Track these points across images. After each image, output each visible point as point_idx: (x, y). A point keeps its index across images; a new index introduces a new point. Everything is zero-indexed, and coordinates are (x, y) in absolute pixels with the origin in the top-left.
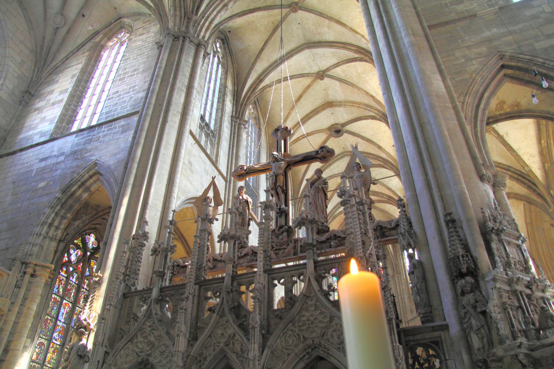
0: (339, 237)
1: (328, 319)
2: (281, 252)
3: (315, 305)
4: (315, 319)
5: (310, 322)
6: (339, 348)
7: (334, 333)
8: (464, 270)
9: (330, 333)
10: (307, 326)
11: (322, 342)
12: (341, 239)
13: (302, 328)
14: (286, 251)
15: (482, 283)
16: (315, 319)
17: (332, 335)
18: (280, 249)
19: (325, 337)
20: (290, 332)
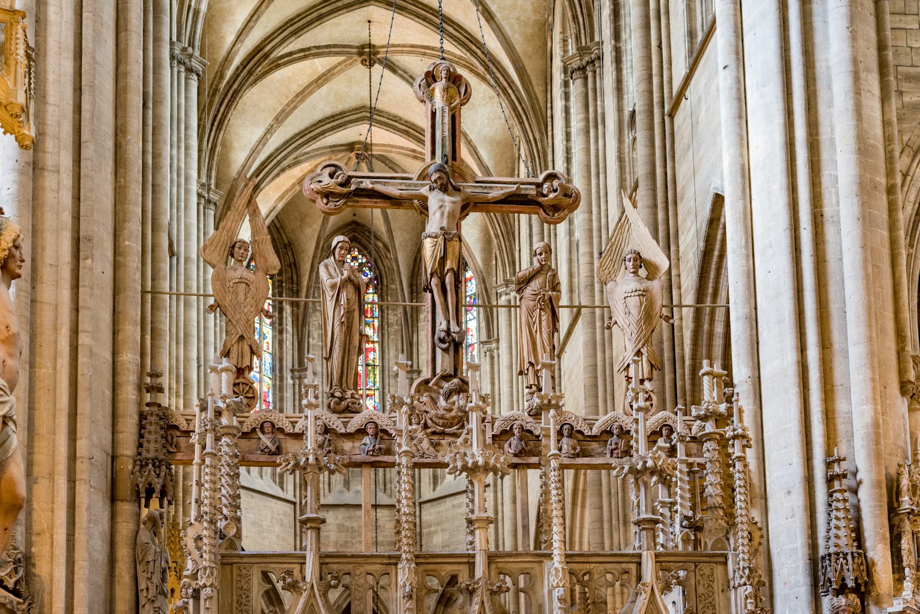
0: (580, 432)
2: (443, 442)
12: (580, 437)
18: (443, 434)
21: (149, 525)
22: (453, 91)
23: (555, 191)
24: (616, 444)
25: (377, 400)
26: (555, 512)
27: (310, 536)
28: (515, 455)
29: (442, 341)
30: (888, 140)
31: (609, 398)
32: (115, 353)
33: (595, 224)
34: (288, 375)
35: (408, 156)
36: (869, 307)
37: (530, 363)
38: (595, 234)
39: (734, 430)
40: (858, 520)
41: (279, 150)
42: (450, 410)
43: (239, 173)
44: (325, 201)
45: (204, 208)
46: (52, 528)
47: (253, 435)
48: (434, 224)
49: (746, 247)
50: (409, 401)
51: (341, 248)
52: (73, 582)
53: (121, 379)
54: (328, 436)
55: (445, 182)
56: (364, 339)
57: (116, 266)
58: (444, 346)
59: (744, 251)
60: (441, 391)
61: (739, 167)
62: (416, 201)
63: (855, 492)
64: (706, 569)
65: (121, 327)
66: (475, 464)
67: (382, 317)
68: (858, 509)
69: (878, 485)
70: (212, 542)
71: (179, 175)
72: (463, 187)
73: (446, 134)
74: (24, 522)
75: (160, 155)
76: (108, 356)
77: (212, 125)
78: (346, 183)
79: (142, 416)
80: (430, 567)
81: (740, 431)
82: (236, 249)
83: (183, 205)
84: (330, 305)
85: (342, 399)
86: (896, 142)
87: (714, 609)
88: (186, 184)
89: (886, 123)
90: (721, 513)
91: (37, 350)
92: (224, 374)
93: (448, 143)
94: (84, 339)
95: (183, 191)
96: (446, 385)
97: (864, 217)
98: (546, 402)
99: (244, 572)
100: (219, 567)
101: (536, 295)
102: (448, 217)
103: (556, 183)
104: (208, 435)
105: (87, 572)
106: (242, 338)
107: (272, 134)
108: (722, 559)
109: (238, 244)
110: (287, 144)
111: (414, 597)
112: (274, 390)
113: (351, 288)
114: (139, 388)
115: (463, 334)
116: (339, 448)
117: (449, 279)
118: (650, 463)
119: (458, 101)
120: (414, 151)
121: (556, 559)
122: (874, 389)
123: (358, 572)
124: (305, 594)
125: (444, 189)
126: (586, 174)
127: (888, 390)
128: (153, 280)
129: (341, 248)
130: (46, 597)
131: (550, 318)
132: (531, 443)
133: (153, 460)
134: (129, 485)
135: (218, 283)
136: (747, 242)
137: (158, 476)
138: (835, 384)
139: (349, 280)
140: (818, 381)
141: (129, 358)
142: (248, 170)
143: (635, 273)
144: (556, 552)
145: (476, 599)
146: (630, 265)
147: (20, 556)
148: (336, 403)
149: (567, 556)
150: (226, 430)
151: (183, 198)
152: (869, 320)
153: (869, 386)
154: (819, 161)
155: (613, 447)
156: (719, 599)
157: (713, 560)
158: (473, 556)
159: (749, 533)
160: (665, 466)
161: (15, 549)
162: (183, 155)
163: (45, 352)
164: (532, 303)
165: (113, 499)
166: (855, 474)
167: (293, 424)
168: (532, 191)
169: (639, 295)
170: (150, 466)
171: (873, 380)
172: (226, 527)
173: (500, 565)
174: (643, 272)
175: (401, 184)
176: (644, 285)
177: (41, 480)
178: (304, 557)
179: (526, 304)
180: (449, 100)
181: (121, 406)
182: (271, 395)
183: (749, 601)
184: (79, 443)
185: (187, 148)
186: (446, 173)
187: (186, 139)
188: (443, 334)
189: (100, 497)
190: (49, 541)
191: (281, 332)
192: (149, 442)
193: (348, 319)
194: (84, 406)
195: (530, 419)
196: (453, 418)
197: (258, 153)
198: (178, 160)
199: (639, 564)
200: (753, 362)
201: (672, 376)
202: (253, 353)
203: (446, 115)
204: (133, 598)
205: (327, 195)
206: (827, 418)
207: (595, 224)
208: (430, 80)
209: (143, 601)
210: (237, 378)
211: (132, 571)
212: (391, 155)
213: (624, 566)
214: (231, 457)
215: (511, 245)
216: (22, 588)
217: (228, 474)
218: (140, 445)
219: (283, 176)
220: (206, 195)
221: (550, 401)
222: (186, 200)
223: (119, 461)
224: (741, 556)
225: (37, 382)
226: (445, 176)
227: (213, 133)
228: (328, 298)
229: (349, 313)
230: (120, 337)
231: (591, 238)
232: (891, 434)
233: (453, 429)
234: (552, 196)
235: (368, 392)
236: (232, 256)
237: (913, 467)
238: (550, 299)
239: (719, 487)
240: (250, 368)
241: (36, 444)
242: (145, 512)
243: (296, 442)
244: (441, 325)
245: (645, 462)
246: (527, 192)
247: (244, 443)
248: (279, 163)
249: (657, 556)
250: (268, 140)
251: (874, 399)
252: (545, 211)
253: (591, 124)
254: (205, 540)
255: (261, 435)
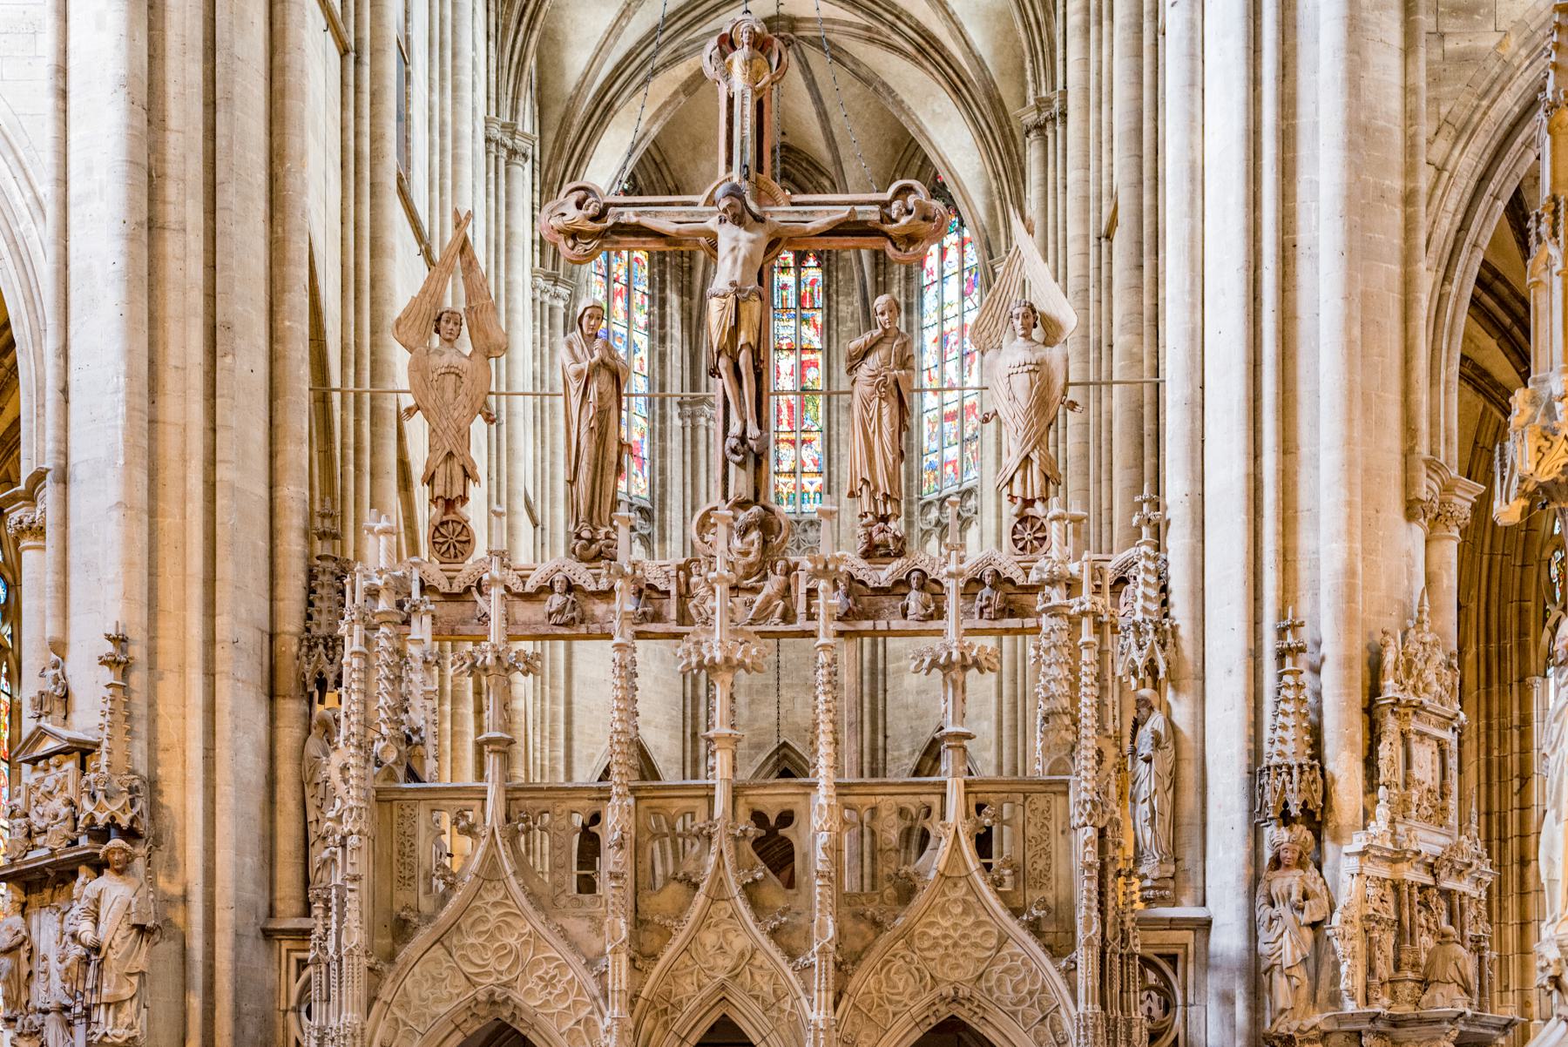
1: (994, 941)
3: (965, 901)
4: (964, 936)
5: (949, 942)
6: (1014, 1013)
7: (1007, 978)
8: (1295, 811)
9: (995, 977)
10: (942, 951)
11: (977, 995)
12: (937, 588)
13: (928, 954)
14: (759, 598)
15: (1329, 846)
16: (964, 936)
17: (999, 980)
19: (983, 984)
20: (899, 962)
21: (320, 731)
22: (760, 62)
23: (909, 212)
24: (988, 598)
25: (819, 449)
26: (822, 727)
27: (492, 763)
28: (839, 619)
29: (734, 451)
30: (1410, 116)
31: (1104, 477)
32: (272, 486)
33: (1093, 189)
34: (673, 411)
35: (859, 37)
36: (1351, 391)
37: (865, 481)
38: (1092, 204)
39: (1081, 604)
40: (1319, 713)
41: (643, 42)
42: (747, 554)
43: (579, 87)
44: (570, 243)
45: (507, 163)
46: (183, 740)
47: (467, 597)
48: (726, 273)
49: (1192, 292)
50: (629, 570)
51: (590, 317)
52: (214, 814)
53: (280, 523)
54: (571, 597)
55: (739, 211)
56: (626, 450)
57: (273, 358)
58: (738, 458)
59: (1188, 299)
60: (736, 525)
61: (1186, 165)
62: (702, 240)
63: (1316, 671)
64: (1040, 802)
65: (279, 447)
66: (712, 659)
67: (829, 307)
68: (1318, 695)
69: (1348, 663)
70: (361, 773)
71: (442, 134)
72: (772, 215)
73: (748, 132)
74: (144, 734)
75: (382, 136)
76: (262, 491)
77: (520, 22)
78: (600, 216)
79: (311, 575)
80: (655, 802)
81: (1088, 606)
82: (443, 323)
83: (449, 183)
84: (575, 402)
85: (592, 541)
86: (1423, 119)
87: (1049, 857)
88: (454, 148)
89: (1408, 90)
90: (1067, 720)
91: (160, 491)
92: (382, 538)
93: (750, 147)
94: (222, 472)
95: (449, 161)
96: (743, 516)
97: (1351, 250)
98: (820, 567)
99: (408, 811)
100: (375, 806)
101: (875, 376)
102: (744, 264)
103: (911, 199)
104: (356, 627)
105: (233, 801)
106: (450, 455)
107: (629, 19)
108: (1062, 788)
109: (444, 317)
110: (656, 30)
111: (629, 844)
112: (651, 438)
113: (605, 376)
114: (307, 534)
115: (764, 442)
116: (588, 613)
117: (744, 359)
118: (956, 656)
119: (767, 78)
120: (868, 29)
121: (822, 791)
122: (1350, 517)
123: (558, 811)
124: (483, 843)
125: (738, 220)
126: (1082, 103)
127: (1382, 515)
128: (373, 332)
129: (590, 317)
130: (177, 835)
131: (896, 411)
132: (865, 599)
133: (325, 639)
134: (293, 675)
135: (418, 376)
136: (1193, 283)
137: (331, 661)
138: (1300, 508)
139: (602, 364)
140: (1274, 503)
141: (294, 492)
142: (595, 77)
143: (1027, 336)
144: (822, 782)
145: (714, 848)
146: (1018, 323)
147: (137, 783)
148: (584, 548)
149: (838, 785)
150: (384, 618)
151: (449, 171)
152: (1350, 410)
153: (1344, 511)
154: (1294, 160)
155: (984, 603)
156: (1057, 844)
157: (1049, 788)
158: (713, 788)
159: (1100, 753)
160: (982, 657)
161: (131, 772)
162: (449, 101)
163: (170, 492)
164: (868, 389)
165: (272, 695)
166: (1318, 644)
167: (524, 579)
168: (872, 215)
169: (1029, 371)
170: (321, 647)
171: (1350, 504)
172: (383, 751)
173: (751, 799)
174: (1037, 334)
175: (680, 213)
176: (1038, 355)
177: (168, 675)
178: (485, 791)
179: (863, 389)
180: (754, 79)
181: (280, 561)
182: (646, 446)
183: (1089, 848)
184: (218, 620)
185: (455, 89)
186: (741, 198)
187: (453, 74)
188: (733, 442)
189: (252, 694)
190: (180, 760)
191: (663, 340)
192: (320, 612)
193: (600, 422)
194: (224, 568)
195: (863, 564)
196: (751, 565)
197: (608, 52)
198: (442, 110)
199: (944, 795)
200: (1193, 472)
201: (1154, 460)
202: (467, 475)
203: (748, 102)
204: (301, 833)
205: (574, 235)
206: (1285, 560)
207: (1093, 189)
208: (726, 47)
209: (312, 838)
210: (445, 514)
211: (299, 796)
212: (832, 37)
213: (923, 798)
214: (391, 654)
215: (1018, 192)
216: (143, 826)
217: (387, 678)
218: (309, 617)
219: (656, 83)
220: (509, 143)
221: (826, 566)
222: (455, 173)
223: (279, 641)
224: (1083, 784)
225: (161, 537)
226: (738, 202)
227: (520, 37)
228: (573, 392)
229: (602, 414)
230: (279, 462)
231: (1087, 211)
232: (1383, 583)
233: (751, 582)
234: (904, 220)
235: (804, 436)
236: (437, 331)
237: (1412, 632)
238: (896, 382)
239: (1066, 684)
240: (464, 499)
241: (161, 624)
242: (319, 709)
243: (527, 605)
244: (735, 429)
245: (950, 654)
246: (867, 217)
247: (453, 609)
248: (643, 64)
249: (967, 784)
250: (622, 29)
251: (1350, 534)
252: (894, 245)
253: (1093, 18)
254: (352, 772)
255: (477, 596)
